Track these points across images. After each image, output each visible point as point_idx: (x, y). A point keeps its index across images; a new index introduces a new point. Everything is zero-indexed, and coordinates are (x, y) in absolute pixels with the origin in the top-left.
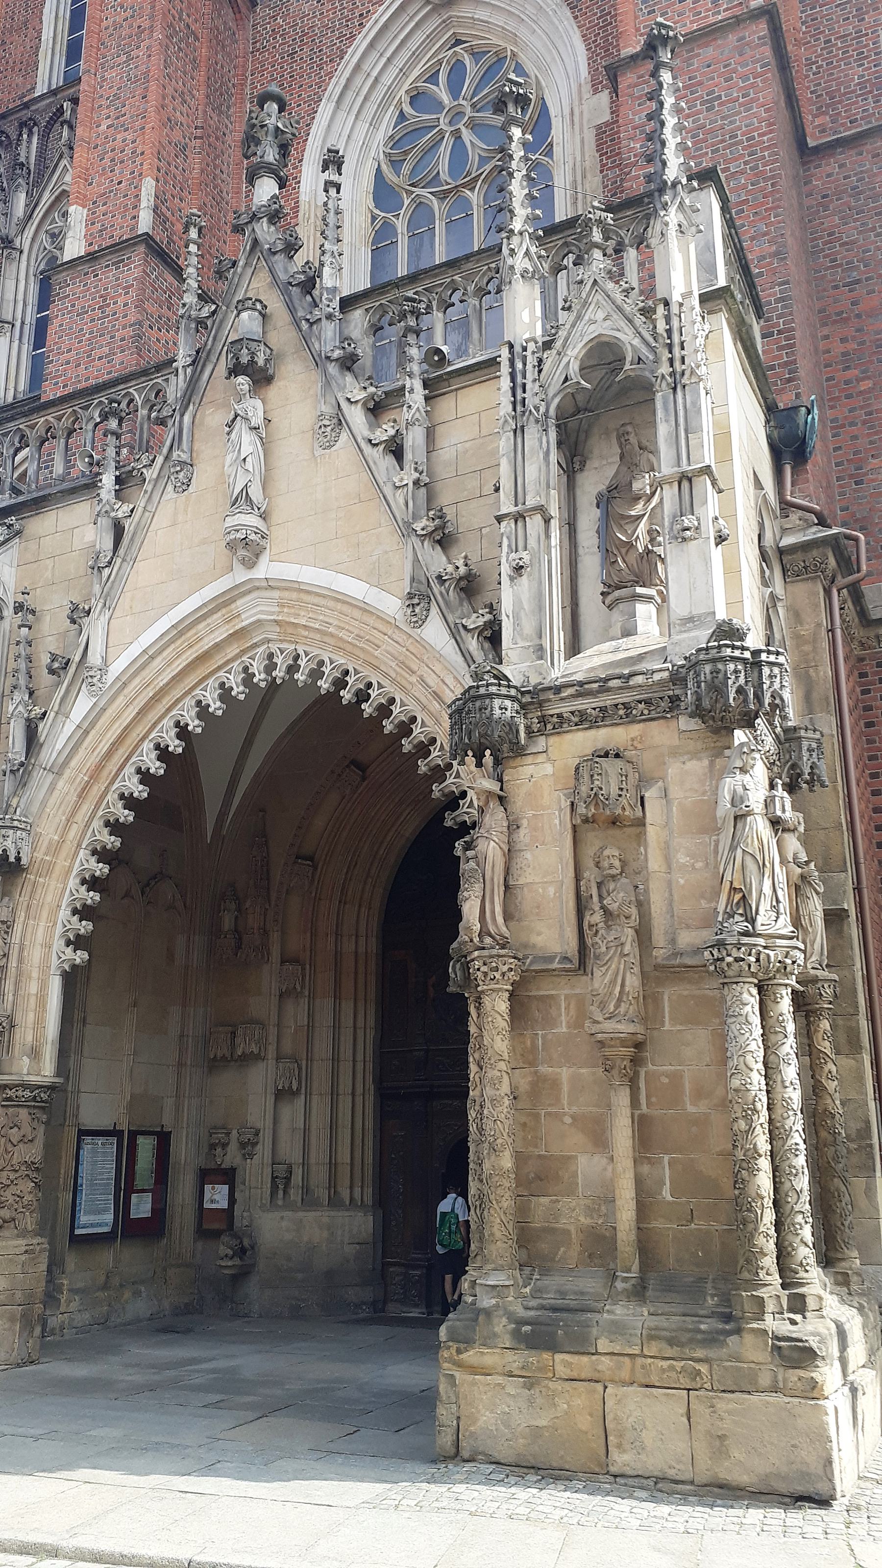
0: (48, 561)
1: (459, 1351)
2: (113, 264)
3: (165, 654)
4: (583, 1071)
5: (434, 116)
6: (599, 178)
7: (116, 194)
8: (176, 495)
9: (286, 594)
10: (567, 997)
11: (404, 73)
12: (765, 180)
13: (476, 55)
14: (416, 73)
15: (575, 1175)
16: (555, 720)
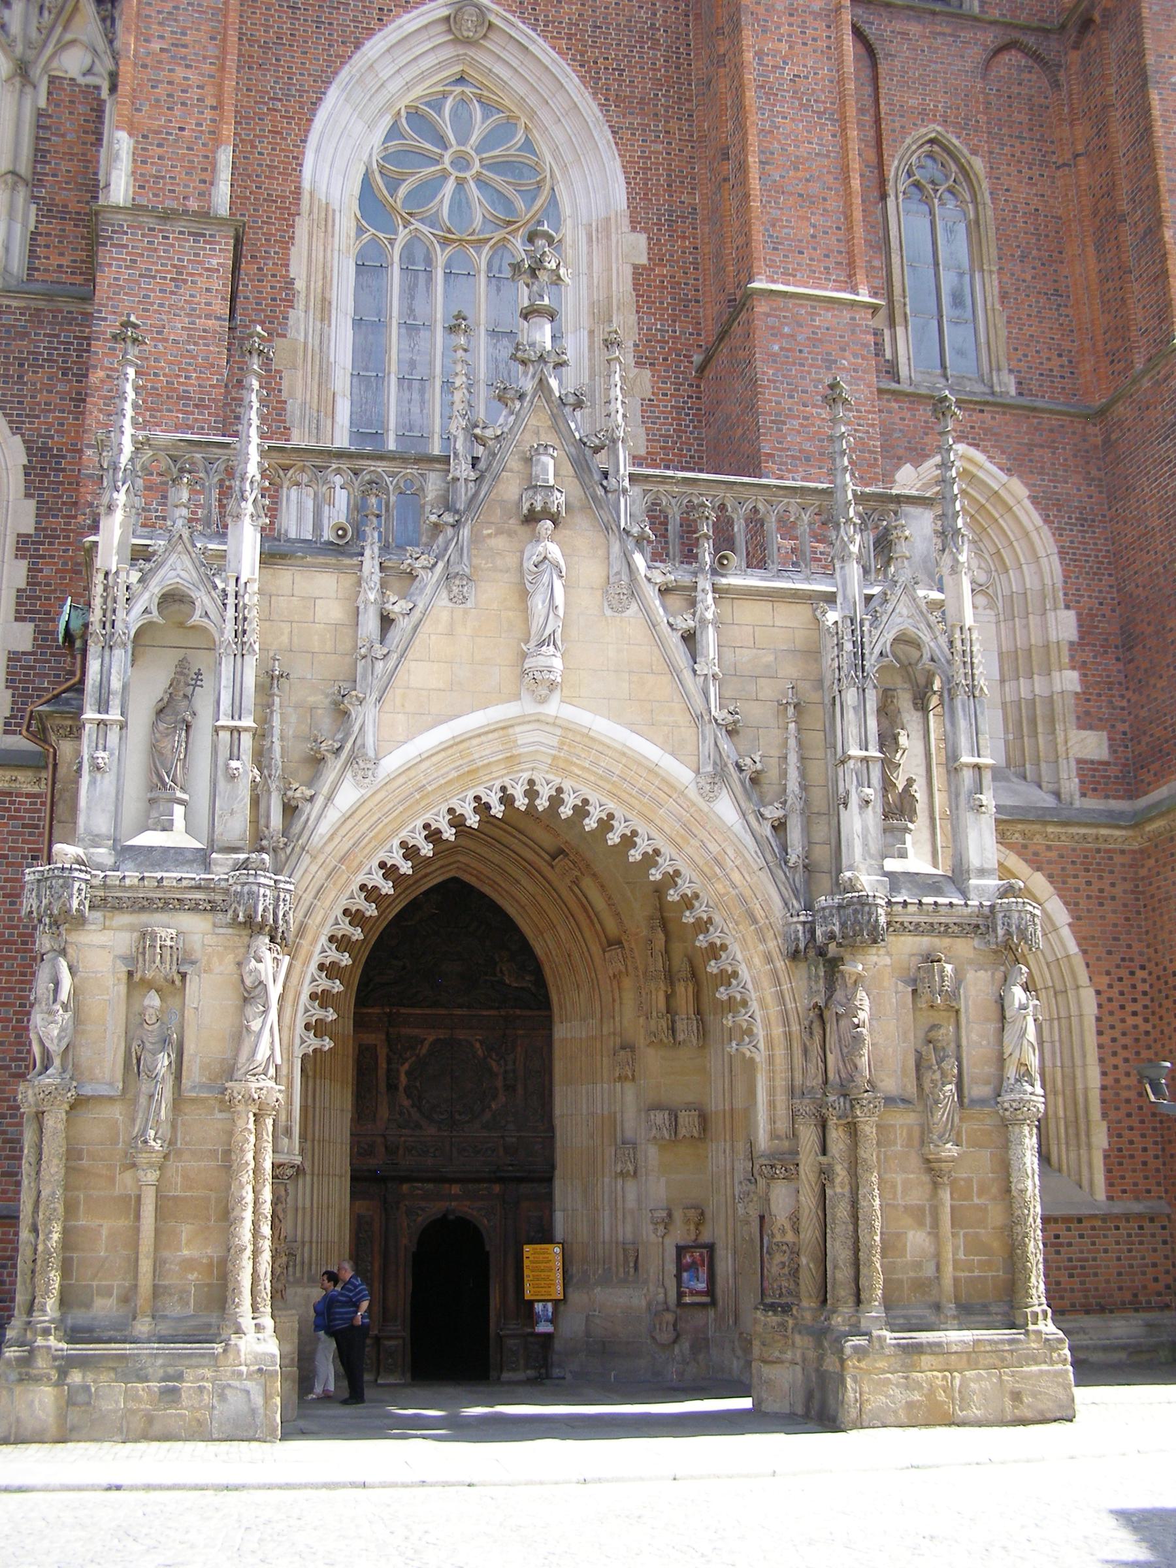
0: (283, 625)
1: (859, 1361)
2: (190, 234)
3: (435, 759)
4: (912, 1176)
5: (439, 151)
6: (633, 318)
7: (176, 141)
8: (451, 605)
9: (570, 735)
10: (902, 1126)
11: (408, 87)
12: (870, 452)
13: (488, 107)
14: (418, 91)
15: (905, 1245)
16: (898, 925)
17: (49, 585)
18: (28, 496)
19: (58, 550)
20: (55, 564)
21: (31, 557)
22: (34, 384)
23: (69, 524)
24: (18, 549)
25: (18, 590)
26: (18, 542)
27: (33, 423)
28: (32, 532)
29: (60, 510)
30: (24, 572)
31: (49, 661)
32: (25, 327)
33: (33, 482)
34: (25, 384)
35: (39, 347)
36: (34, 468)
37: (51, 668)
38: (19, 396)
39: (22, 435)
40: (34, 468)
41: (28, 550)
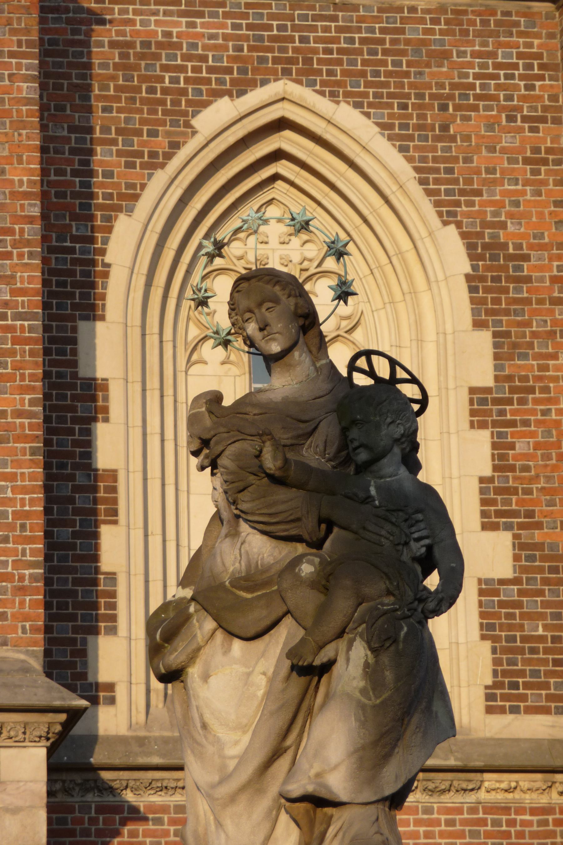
17: (526, 469)
18: (478, 324)
19: (533, 412)
20: (533, 435)
21: (495, 424)
22: (467, 138)
23: (545, 368)
24: (473, 413)
25: (482, 480)
26: (471, 402)
27: (471, 204)
28: (489, 382)
29: (531, 345)
30: (486, 450)
31: (541, 593)
32: (442, 43)
33: (483, 301)
34: (453, 139)
35: (467, 76)
36: (483, 279)
37: (545, 604)
38: (445, 160)
39: (459, 225)
40: (483, 279)
41: (489, 413)
